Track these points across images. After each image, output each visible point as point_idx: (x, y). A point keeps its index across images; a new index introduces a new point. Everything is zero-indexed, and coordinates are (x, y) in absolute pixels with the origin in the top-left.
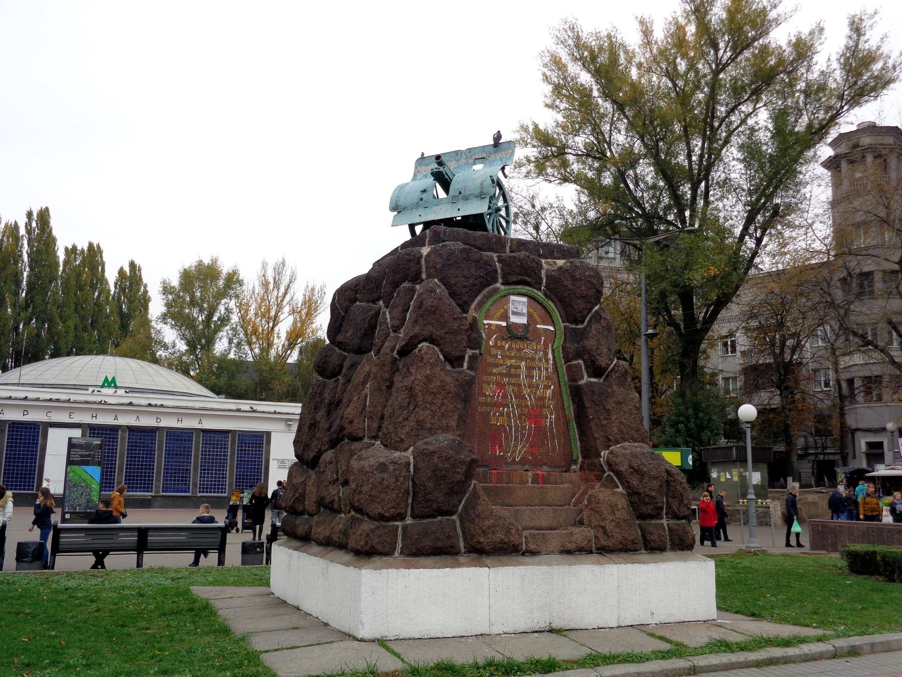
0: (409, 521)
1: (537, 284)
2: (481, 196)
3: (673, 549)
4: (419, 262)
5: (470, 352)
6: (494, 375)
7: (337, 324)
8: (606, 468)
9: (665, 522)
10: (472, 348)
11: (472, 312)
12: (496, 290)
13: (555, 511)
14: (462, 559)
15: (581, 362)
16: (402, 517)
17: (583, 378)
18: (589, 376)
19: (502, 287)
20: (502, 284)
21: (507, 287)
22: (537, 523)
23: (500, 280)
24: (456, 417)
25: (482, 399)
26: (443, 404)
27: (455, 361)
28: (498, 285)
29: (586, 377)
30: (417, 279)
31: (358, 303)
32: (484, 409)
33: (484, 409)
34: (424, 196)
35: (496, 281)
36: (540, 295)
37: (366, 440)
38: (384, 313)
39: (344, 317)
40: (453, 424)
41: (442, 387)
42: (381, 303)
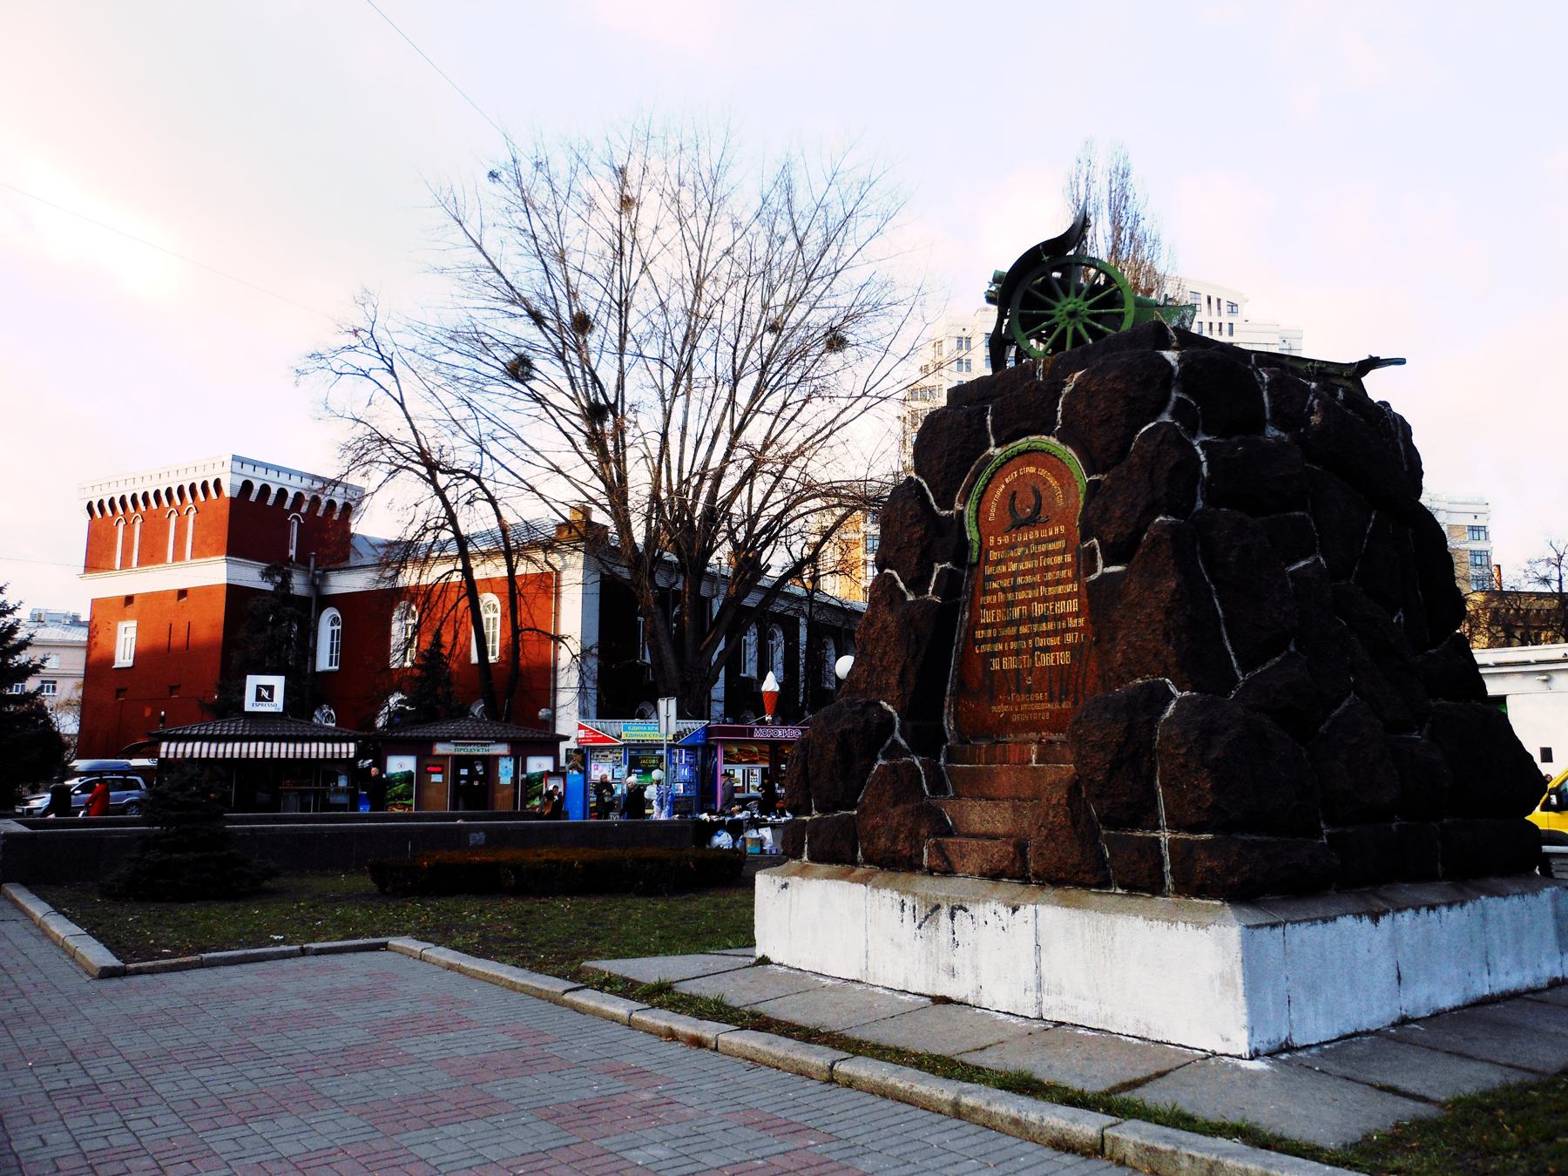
0: (816, 815)
1: (1046, 428)
3: (1178, 892)
5: (938, 567)
6: (994, 592)
9: (1165, 836)
11: (958, 507)
13: (1015, 809)
14: (860, 871)
16: (809, 814)
18: (1106, 565)
19: (998, 451)
20: (997, 446)
22: (989, 827)
23: (993, 442)
24: (898, 670)
25: (979, 634)
26: (885, 653)
27: (918, 584)
28: (991, 450)
29: (1100, 563)
32: (987, 648)
33: (987, 648)
40: (893, 680)
41: (884, 628)
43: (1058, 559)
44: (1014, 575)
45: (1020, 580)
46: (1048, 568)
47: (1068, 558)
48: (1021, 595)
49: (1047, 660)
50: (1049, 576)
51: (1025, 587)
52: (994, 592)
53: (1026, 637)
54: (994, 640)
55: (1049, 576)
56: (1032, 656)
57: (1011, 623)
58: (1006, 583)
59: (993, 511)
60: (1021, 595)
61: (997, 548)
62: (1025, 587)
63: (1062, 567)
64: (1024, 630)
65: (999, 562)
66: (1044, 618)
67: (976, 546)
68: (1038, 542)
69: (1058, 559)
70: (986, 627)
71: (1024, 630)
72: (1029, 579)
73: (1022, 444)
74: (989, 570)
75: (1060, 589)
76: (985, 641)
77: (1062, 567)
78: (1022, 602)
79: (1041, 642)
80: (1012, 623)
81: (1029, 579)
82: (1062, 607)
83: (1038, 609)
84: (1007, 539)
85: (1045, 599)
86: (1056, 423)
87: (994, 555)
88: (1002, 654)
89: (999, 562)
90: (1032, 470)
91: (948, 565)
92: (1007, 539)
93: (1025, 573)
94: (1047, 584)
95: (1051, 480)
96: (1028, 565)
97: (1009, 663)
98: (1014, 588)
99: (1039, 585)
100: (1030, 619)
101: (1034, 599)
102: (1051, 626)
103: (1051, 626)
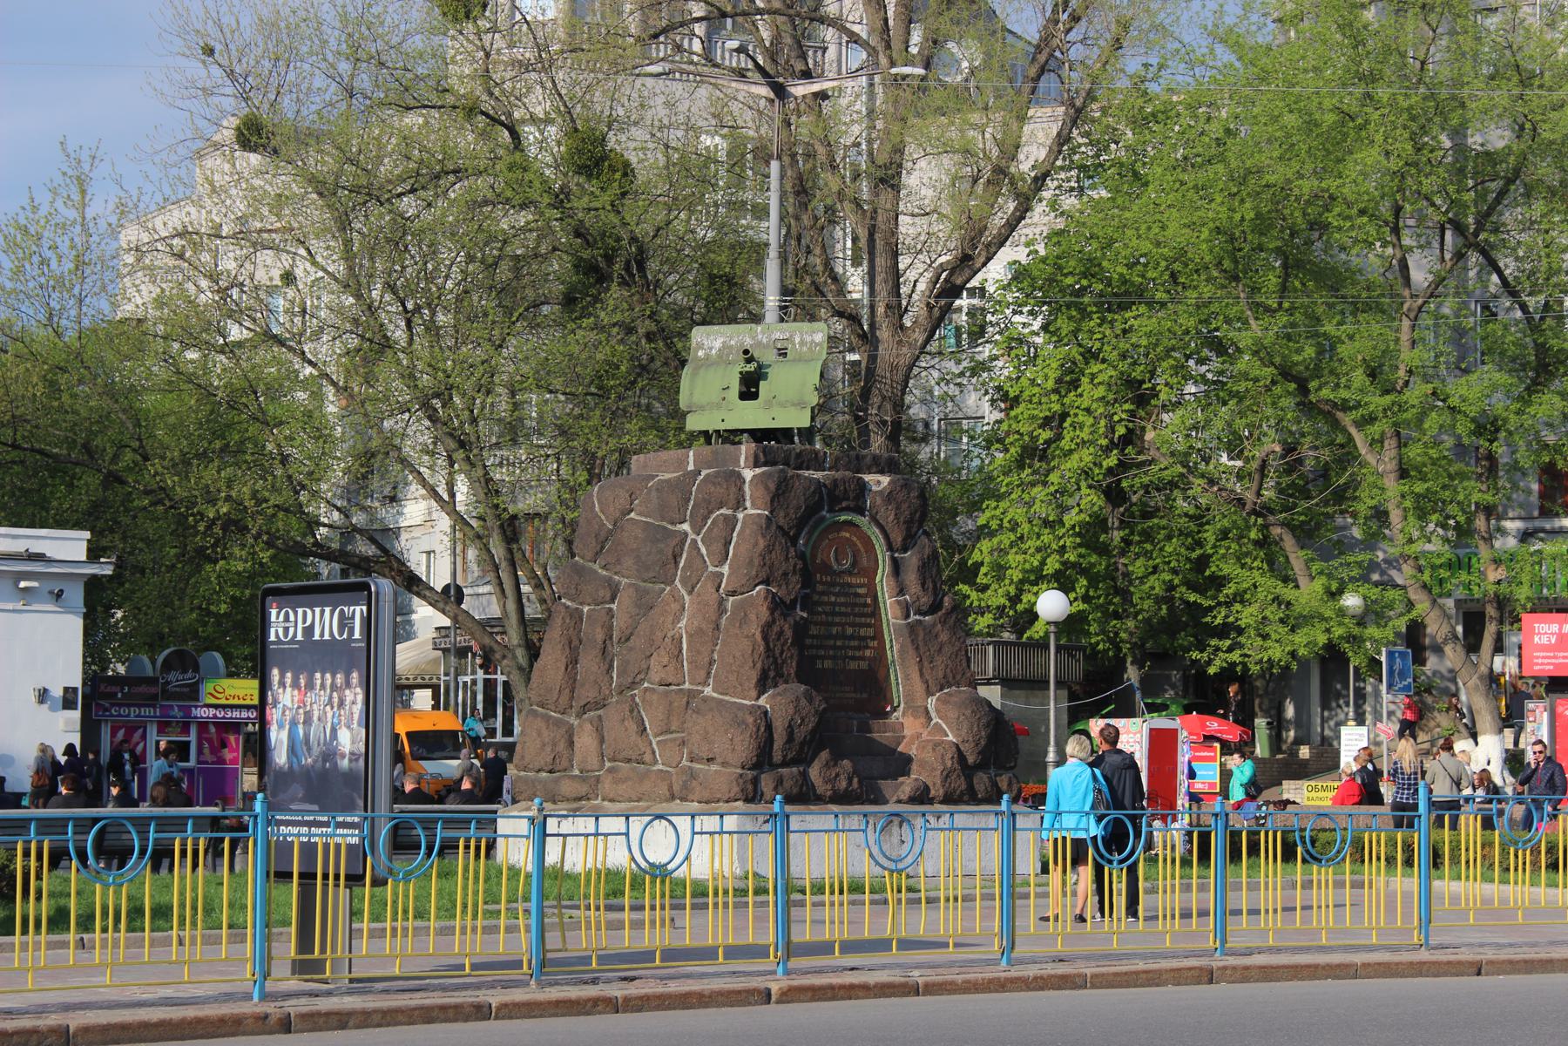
2: (800, 405)
4: (741, 489)
7: (602, 538)
8: (933, 714)
12: (823, 518)
17: (907, 616)
25: (808, 641)
30: (739, 504)
31: (632, 515)
34: (725, 394)
37: (687, 686)
38: (694, 542)
39: (610, 532)
42: (686, 527)
44: (834, 604)
47: (869, 601)
48: (837, 620)
49: (853, 665)
51: (840, 614)
52: (820, 613)
53: (841, 648)
54: (819, 647)
57: (830, 637)
58: (827, 608)
60: (837, 620)
62: (840, 614)
64: (839, 643)
65: (823, 593)
66: (852, 637)
70: (813, 637)
71: (839, 643)
74: (816, 598)
76: (812, 647)
79: (850, 653)
80: (830, 637)
82: (863, 632)
83: (849, 631)
85: (853, 625)
87: (820, 588)
88: (823, 658)
89: (823, 593)
93: (841, 604)
94: (855, 615)
97: (828, 664)
98: (834, 614)
100: (845, 637)
102: (856, 643)
103: (856, 643)
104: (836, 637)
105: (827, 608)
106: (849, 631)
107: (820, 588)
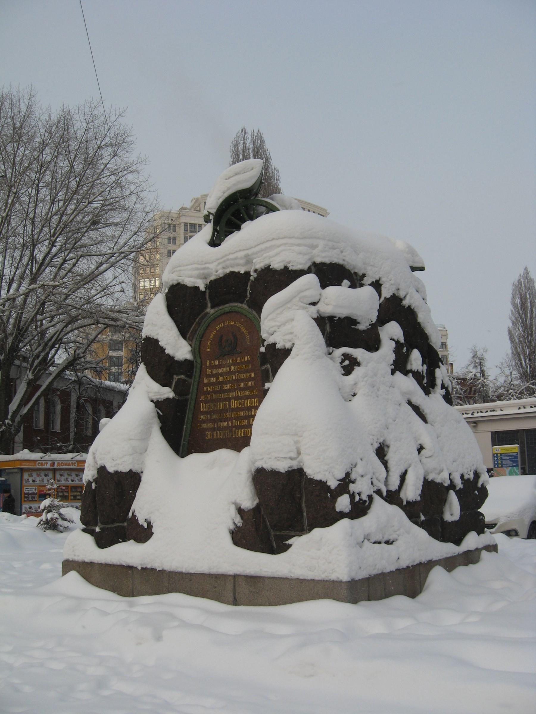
10: (177, 375)
12: (208, 313)
15: (269, 366)
19: (212, 311)
20: (212, 307)
21: (216, 309)
23: (209, 305)
32: (204, 426)
33: (204, 426)
35: (206, 307)
36: (245, 306)
43: (247, 375)
44: (221, 383)
45: (224, 387)
46: (242, 380)
47: (253, 375)
48: (225, 396)
50: (241, 385)
55: (241, 385)
56: (231, 431)
59: (209, 346)
60: (225, 396)
61: (211, 367)
63: (250, 379)
64: (226, 415)
66: (237, 409)
67: (199, 366)
68: (235, 364)
69: (247, 375)
71: (226, 415)
72: (230, 386)
73: (227, 307)
75: (248, 393)
76: (203, 421)
77: (250, 379)
78: (225, 399)
81: (230, 386)
83: (235, 404)
84: (217, 362)
85: (237, 398)
86: (246, 297)
88: (213, 430)
89: (212, 376)
90: (232, 323)
91: (182, 377)
92: (217, 362)
95: (243, 329)
96: (230, 378)
98: (222, 391)
99: (235, 390)
101: (233, 398)
104: (225, 411)
105: (216, 388)
106: (235, 404)
107: (209, 371)
